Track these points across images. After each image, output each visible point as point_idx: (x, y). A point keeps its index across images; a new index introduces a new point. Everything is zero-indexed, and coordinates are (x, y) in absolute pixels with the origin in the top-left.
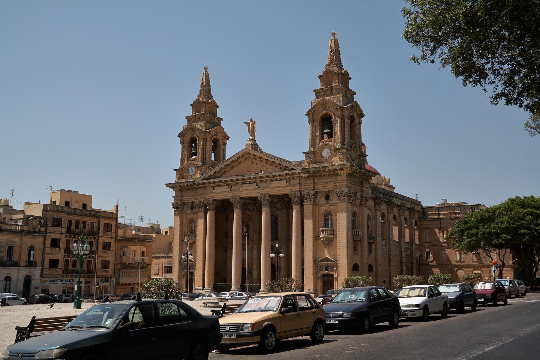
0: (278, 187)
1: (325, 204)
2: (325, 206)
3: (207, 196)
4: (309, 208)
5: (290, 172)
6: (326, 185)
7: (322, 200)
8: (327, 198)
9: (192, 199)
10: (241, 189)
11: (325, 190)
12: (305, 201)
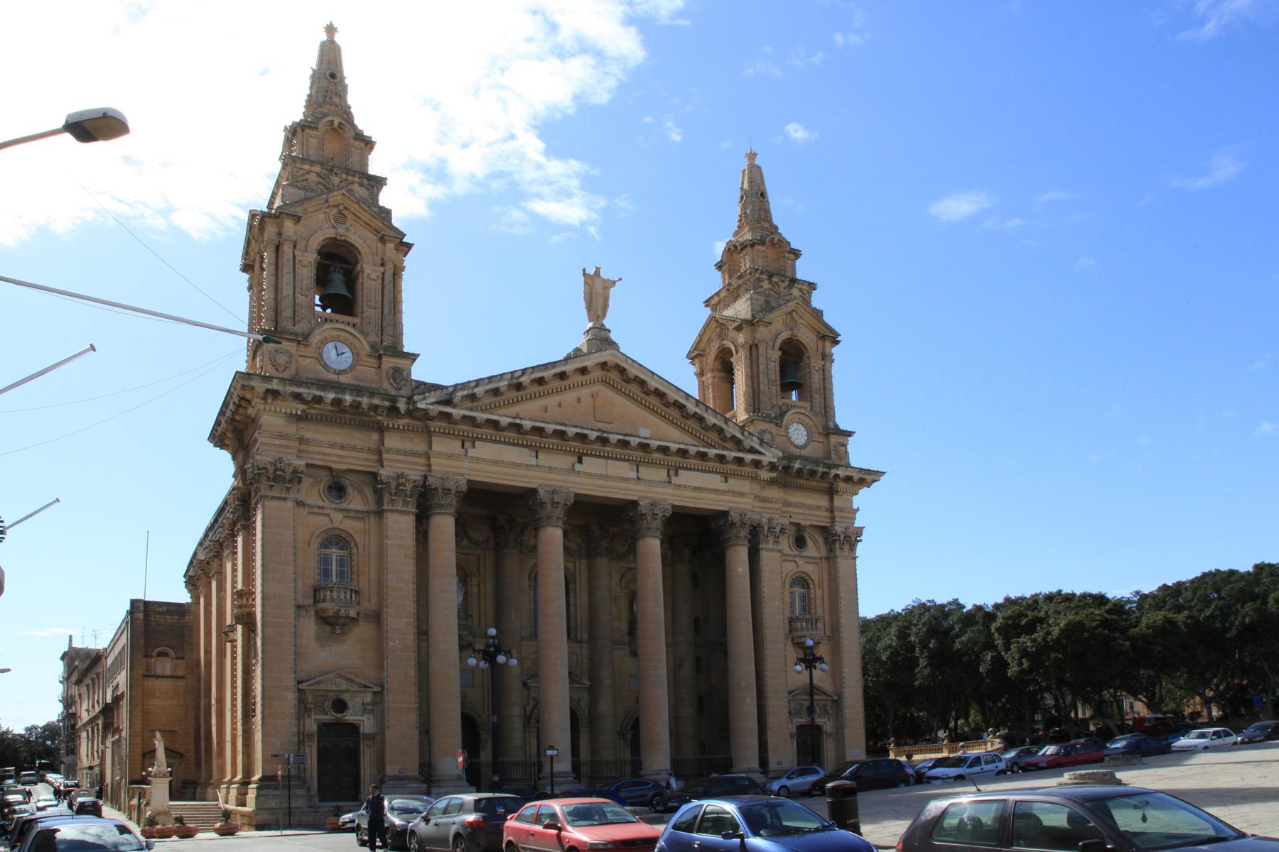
0: (696, 489)
1: (794, 556)
2: (795, 562)
4: (768, 559)
6: (807, 512)
7: (785, 544)
9: (346, 460)
10: (578, 467)
11: (803, 523)
12: (762, 537)
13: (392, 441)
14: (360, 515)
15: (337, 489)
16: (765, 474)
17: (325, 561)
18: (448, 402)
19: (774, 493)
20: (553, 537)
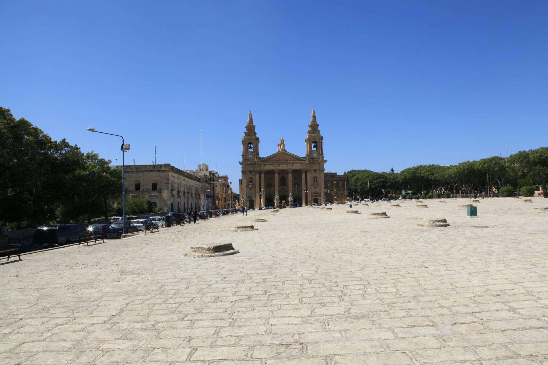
3: (261, 168)
4: (309, 175)
5: (303, 161)
7: (313, 172)
8: (315, 171)
13: (256, 166)
14: (254, 175)
15: (251, 172)
16: (308, 163)
17: (250, 181)
18: (262, 161)
19: (310, 165)
20: (276, 175)
